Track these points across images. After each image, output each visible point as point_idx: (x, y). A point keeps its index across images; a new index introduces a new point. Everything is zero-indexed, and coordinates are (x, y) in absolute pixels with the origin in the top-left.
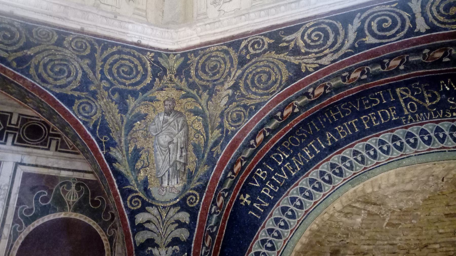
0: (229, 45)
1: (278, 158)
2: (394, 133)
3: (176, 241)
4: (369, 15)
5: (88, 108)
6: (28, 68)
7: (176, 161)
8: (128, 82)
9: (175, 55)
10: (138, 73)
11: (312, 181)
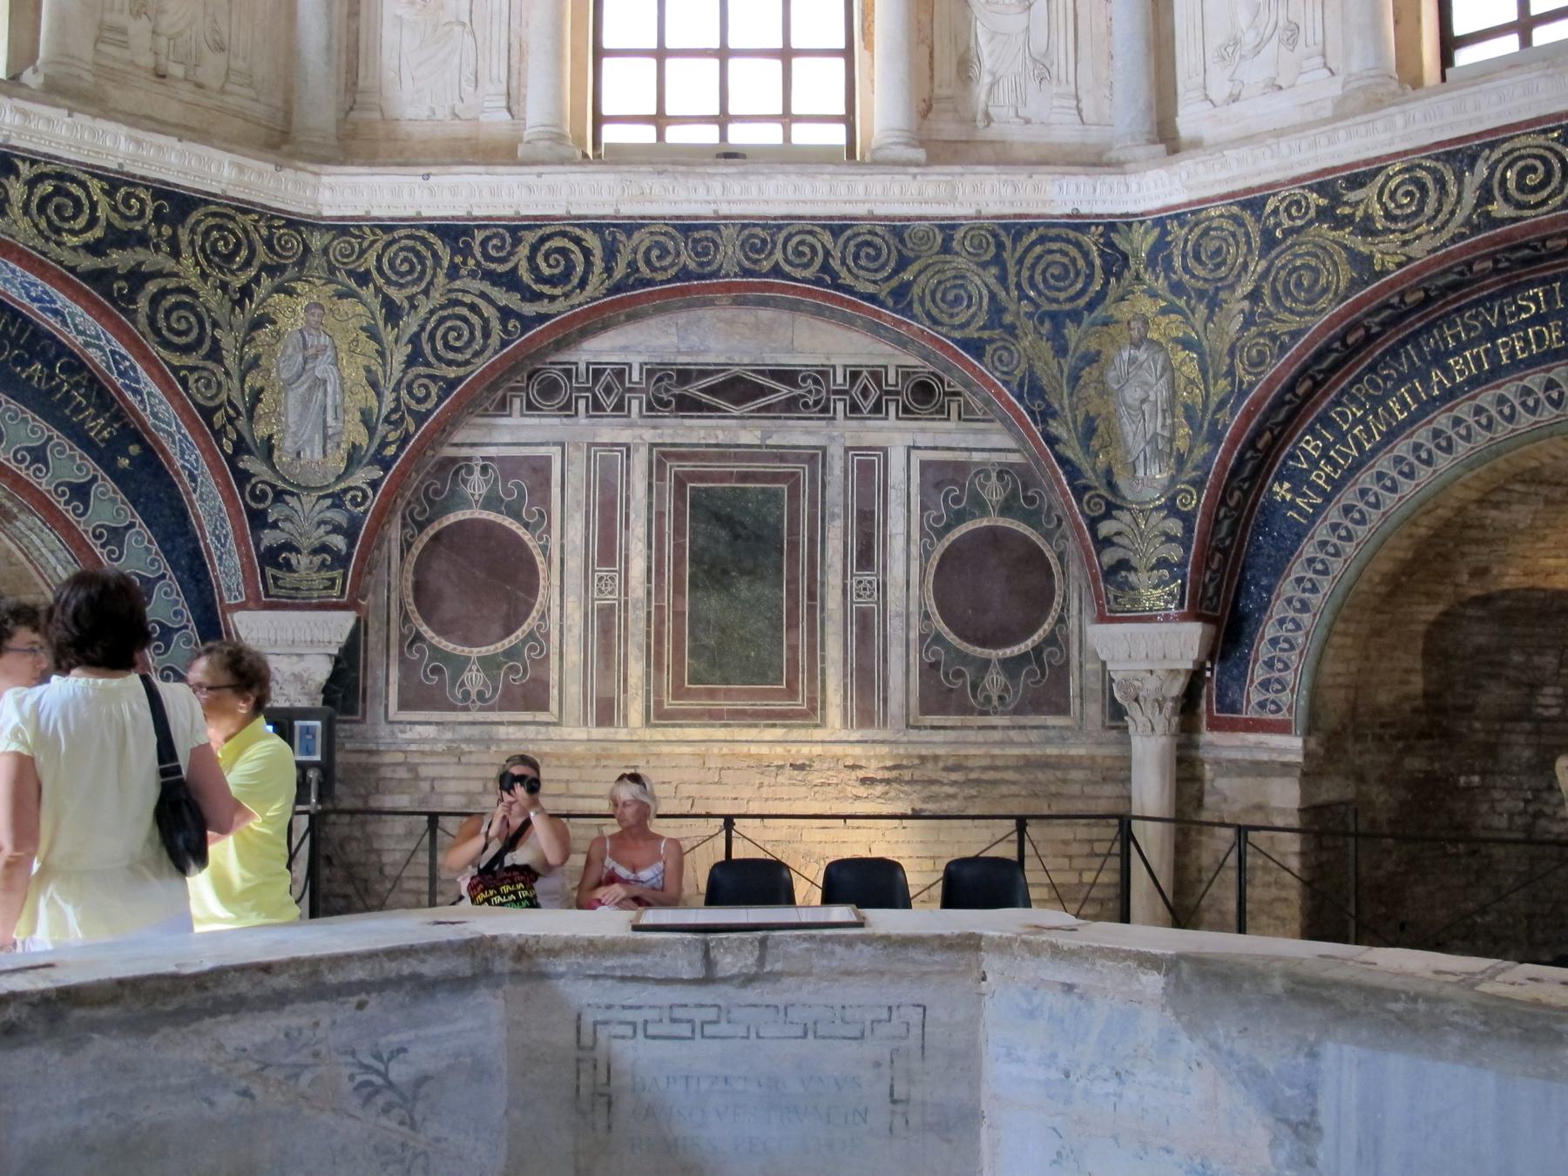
0: (1244, 205)
1: (1343, 415)
2: (1552, 375)
3: (1163, 563)
4: (1505, 154)
5: (1005, 355)
6: (910, 303)
7: (1155, 434)
8: (1062, 296)
9: (1142, 223)
10: (1078, 274)
11: (1399, 460)
